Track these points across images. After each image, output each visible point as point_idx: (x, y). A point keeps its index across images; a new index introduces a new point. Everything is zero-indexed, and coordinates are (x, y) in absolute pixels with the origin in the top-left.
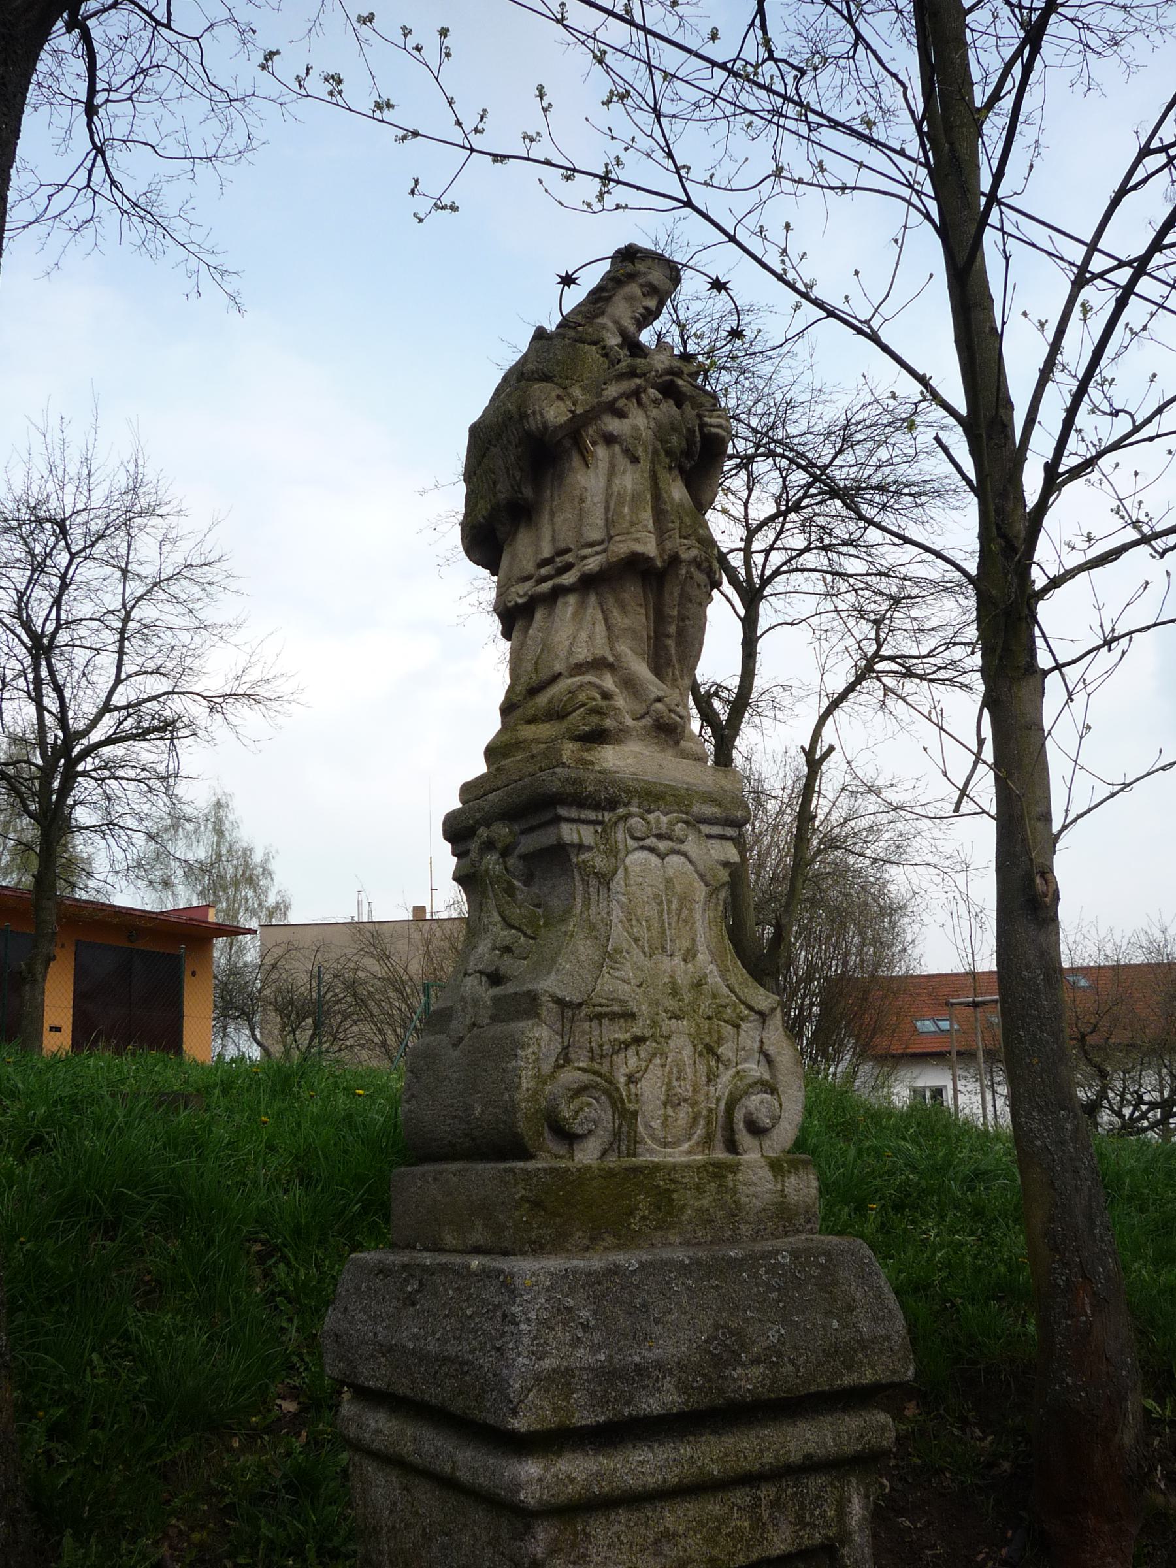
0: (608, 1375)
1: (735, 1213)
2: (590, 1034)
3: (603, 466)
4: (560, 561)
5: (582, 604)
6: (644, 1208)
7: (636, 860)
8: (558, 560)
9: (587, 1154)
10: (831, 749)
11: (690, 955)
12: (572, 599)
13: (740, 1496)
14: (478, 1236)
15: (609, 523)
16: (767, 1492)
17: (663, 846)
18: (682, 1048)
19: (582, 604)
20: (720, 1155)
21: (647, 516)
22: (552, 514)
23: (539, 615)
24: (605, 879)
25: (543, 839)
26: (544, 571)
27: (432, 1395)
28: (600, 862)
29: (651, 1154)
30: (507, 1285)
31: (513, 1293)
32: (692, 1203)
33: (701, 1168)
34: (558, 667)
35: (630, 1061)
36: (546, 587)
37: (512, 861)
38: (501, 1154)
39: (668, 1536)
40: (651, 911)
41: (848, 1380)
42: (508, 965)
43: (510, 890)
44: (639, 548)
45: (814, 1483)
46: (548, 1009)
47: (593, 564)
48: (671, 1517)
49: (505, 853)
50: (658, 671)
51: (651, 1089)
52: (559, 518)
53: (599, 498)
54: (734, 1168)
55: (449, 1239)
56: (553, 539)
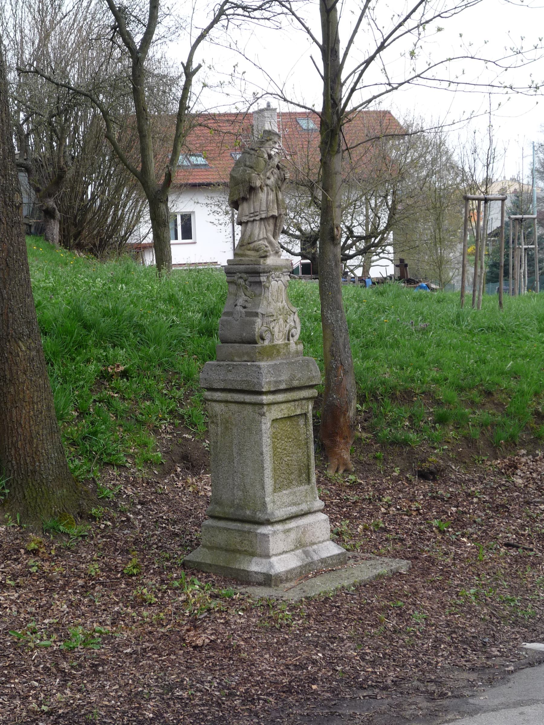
0: (276, 382)
1: (289, 353)
2: (266, 319)
3: (266, 192)
4: (256, 214)
5: (260, 224)
6: (275, 353)
7: (273, 283)
8: (255, 214)
9: (266, 343)
10: (200, 66)
11: (282, 302)
12: (258, 222)
13: (293, 403)
14: (246, 358)
15: (267, 207)
16: (297, 403)
17: (277, 279)
18: (281, 321)
19: (260, 224)
20: (286, 341)
21: (276, 206)
22: (254, 202)
23: (249, 224)
24: (268, 288)
25: (257, 279)
26: (251, 215)
27: (239, 387)
28: (267, 285)
29: (276, 342)
30: (259, 367)
31: (260, 369)
32: (283, 351)
33: (284, 344)
34: (256, 239)
35: (273, 324)
36: (252, 219)
37: (247, 282)
38: (249, 343)
39: (282, 409)
40: (275, 294)
41: (311, 383)
42: (247, 305)
43: (246, 288)
44: (274, 214)
45: (304, 402)
46: (260, 316)
47: (263, 216)
48: (283, 406)
49: (245, 281)
50: (274, 237)
51: (276, 330)
52: (256, 204)
53: (265, 200)
54: (289, 344)
55: (236, 359)
56: (254, 208)
